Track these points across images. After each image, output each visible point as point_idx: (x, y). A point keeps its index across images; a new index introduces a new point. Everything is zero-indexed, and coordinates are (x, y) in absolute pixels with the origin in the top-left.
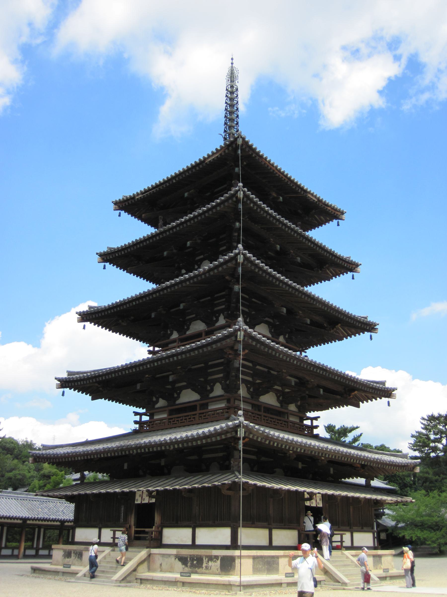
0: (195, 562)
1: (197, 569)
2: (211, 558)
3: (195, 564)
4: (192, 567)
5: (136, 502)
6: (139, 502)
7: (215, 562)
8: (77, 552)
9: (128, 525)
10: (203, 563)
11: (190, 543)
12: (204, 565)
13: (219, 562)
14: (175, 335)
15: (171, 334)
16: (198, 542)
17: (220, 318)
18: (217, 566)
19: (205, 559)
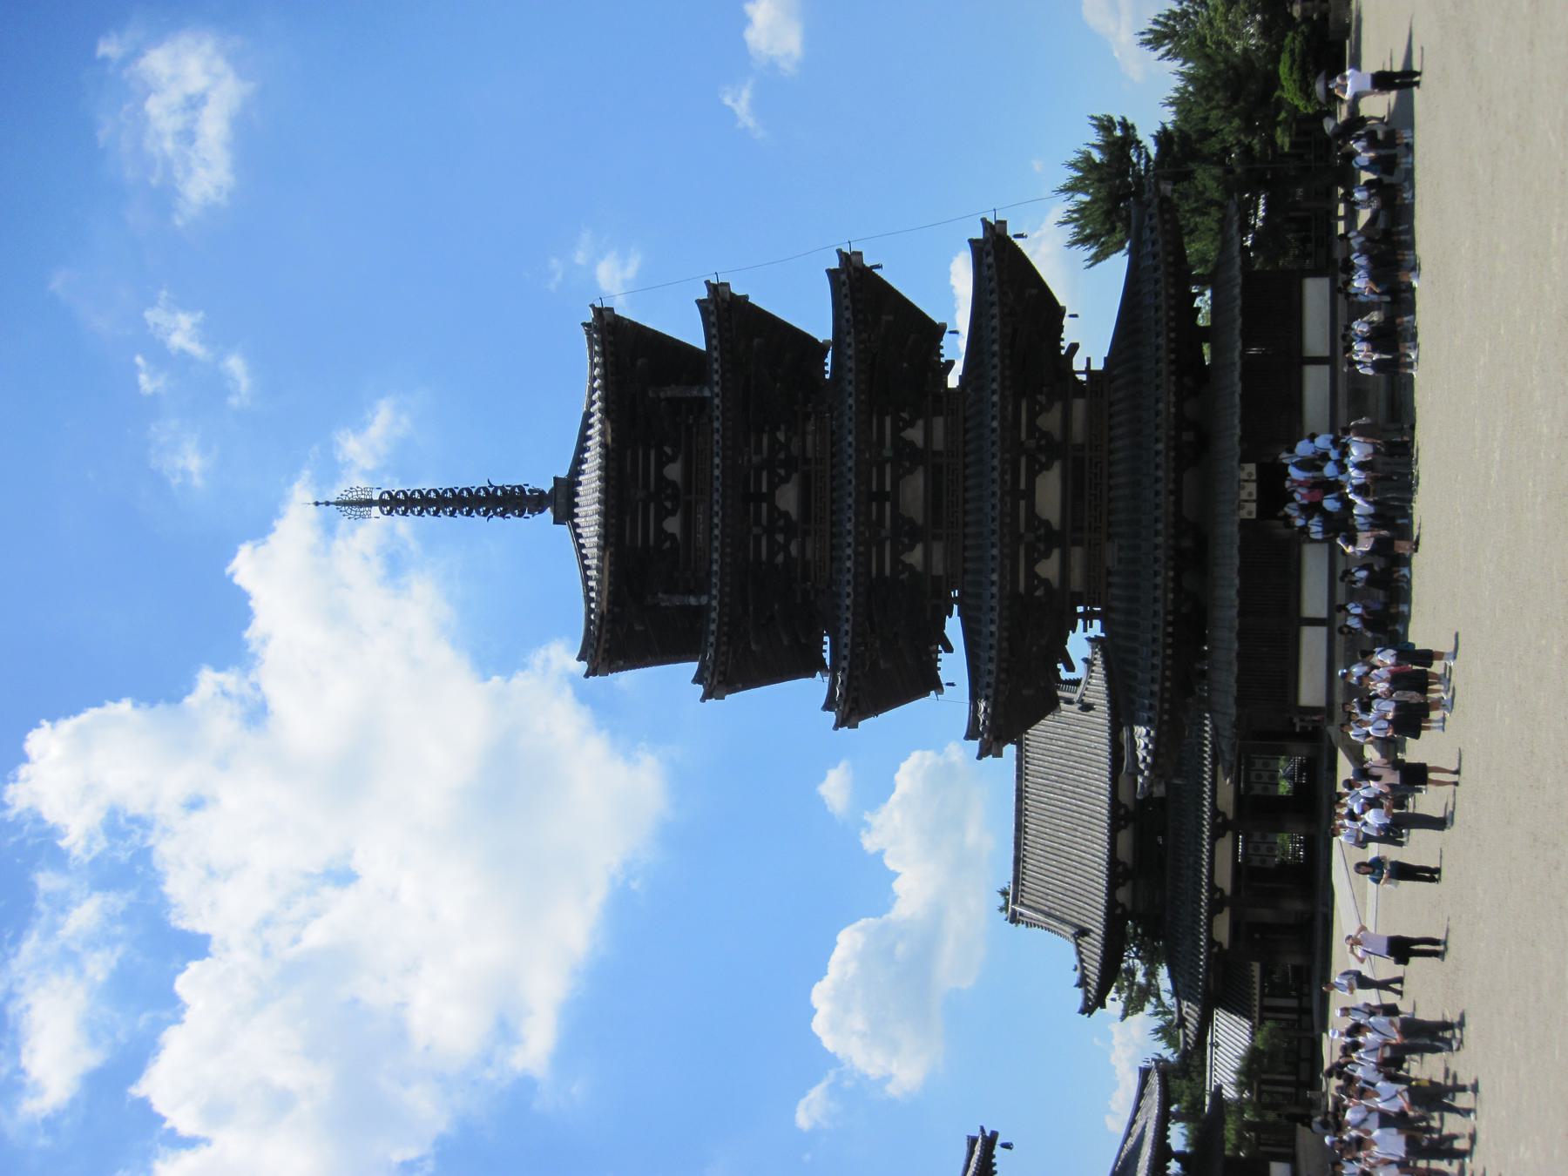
6: (1253, 507)
11: (1326, 369)
15: (911, 567)
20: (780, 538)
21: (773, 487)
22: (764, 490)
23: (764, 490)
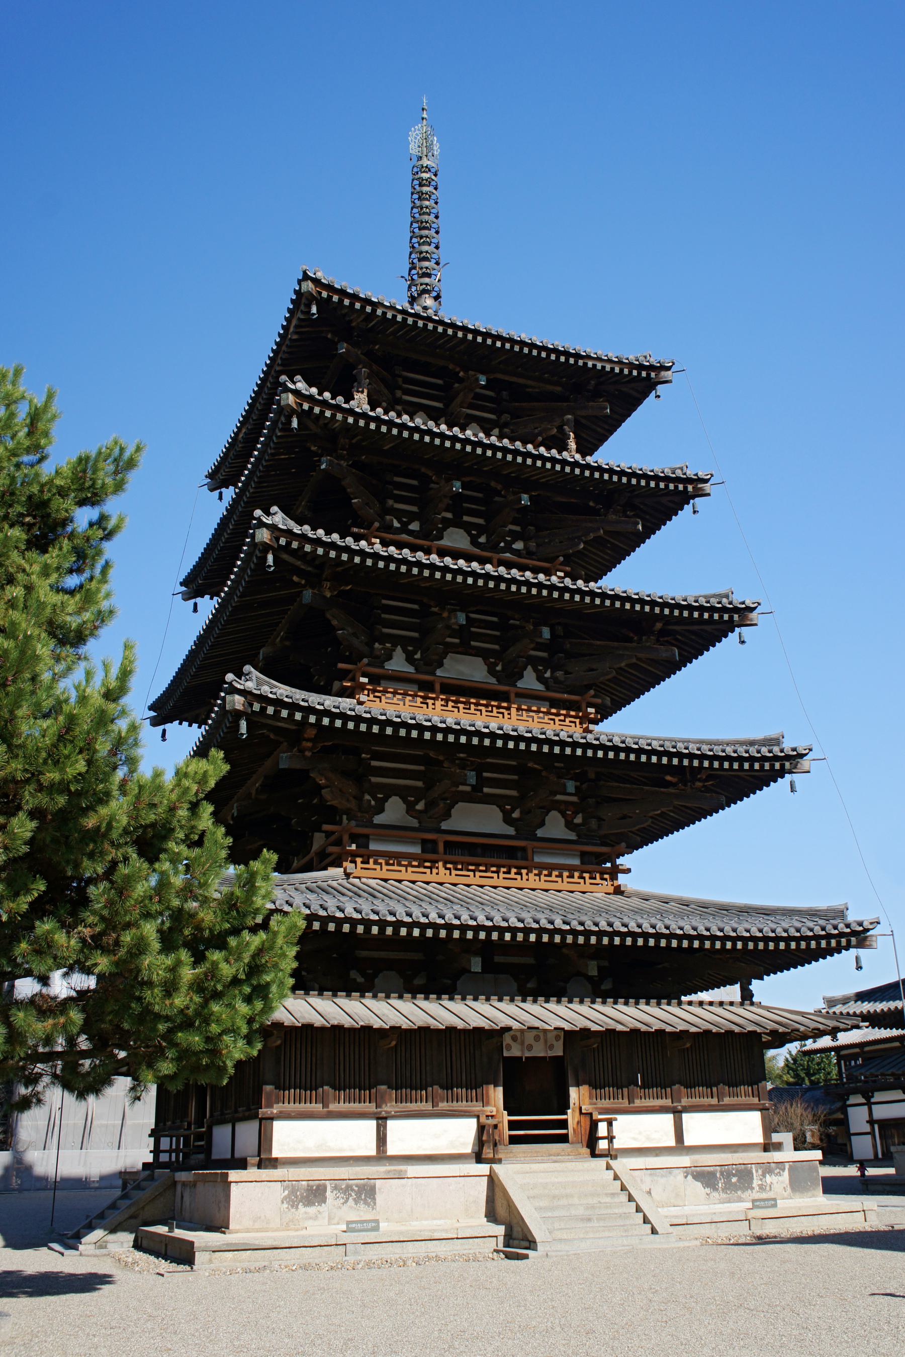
0: (734, 1180)
1: (739, 1193)
2: (768, 1169)
3: (735, 1184)
4: (729, 1189)
5: (506, 1054)
7: (779, 1174)
8: (349, 1187)
9: (494, 1109)
10: (752, 1179)
12: (756, 1183)
13: (786, 1173)
14: (398, 663)
16: (688, 1141)
17: (525, 673)
18: (783, 1182)
19: (757, 1171)
20: (414, 526)
21: (467, 528)
22: (466, 518)
23: (466, 518)
